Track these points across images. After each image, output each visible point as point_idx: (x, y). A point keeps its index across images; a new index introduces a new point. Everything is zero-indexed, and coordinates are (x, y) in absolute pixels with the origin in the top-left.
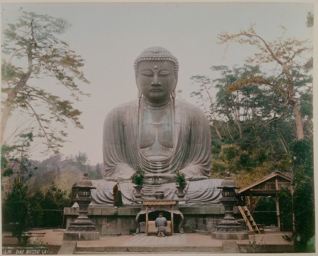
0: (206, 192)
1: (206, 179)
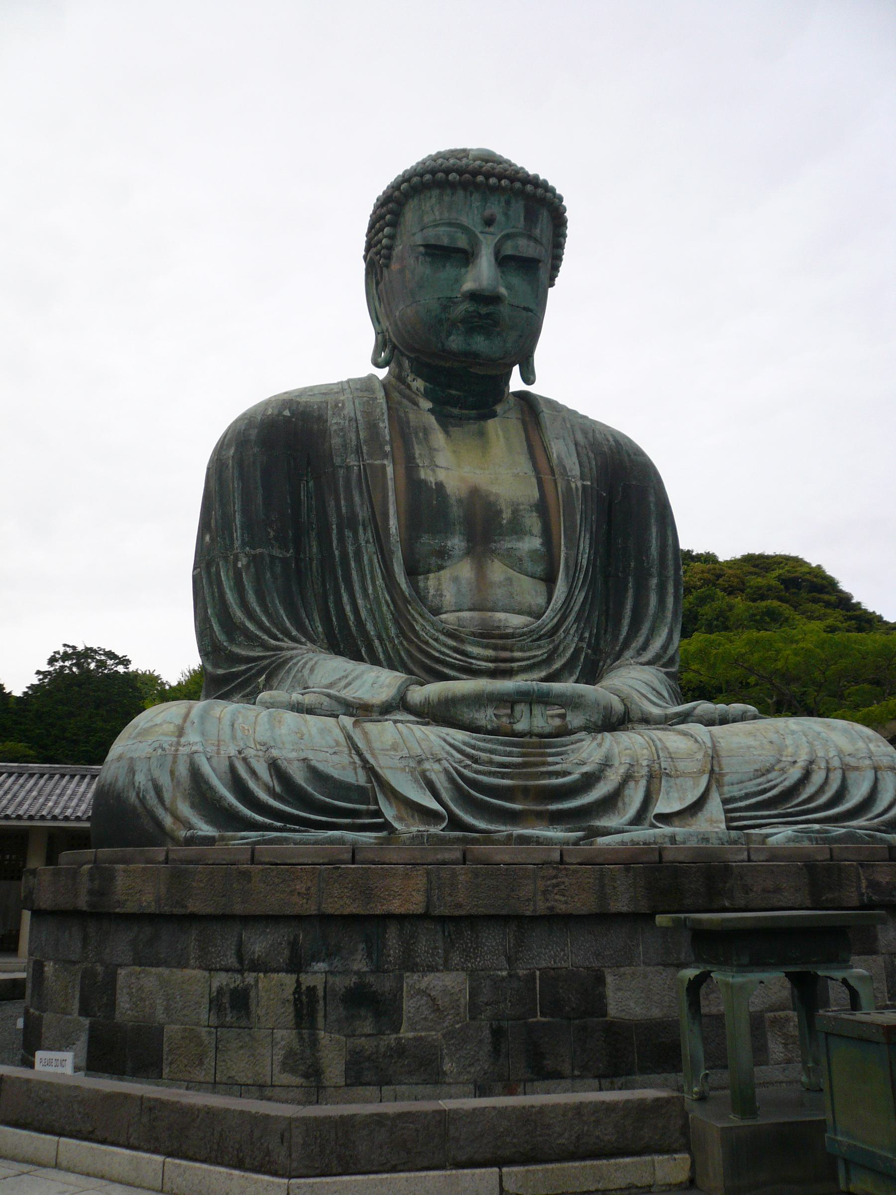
0: (807, 775)
1: (755, 718)
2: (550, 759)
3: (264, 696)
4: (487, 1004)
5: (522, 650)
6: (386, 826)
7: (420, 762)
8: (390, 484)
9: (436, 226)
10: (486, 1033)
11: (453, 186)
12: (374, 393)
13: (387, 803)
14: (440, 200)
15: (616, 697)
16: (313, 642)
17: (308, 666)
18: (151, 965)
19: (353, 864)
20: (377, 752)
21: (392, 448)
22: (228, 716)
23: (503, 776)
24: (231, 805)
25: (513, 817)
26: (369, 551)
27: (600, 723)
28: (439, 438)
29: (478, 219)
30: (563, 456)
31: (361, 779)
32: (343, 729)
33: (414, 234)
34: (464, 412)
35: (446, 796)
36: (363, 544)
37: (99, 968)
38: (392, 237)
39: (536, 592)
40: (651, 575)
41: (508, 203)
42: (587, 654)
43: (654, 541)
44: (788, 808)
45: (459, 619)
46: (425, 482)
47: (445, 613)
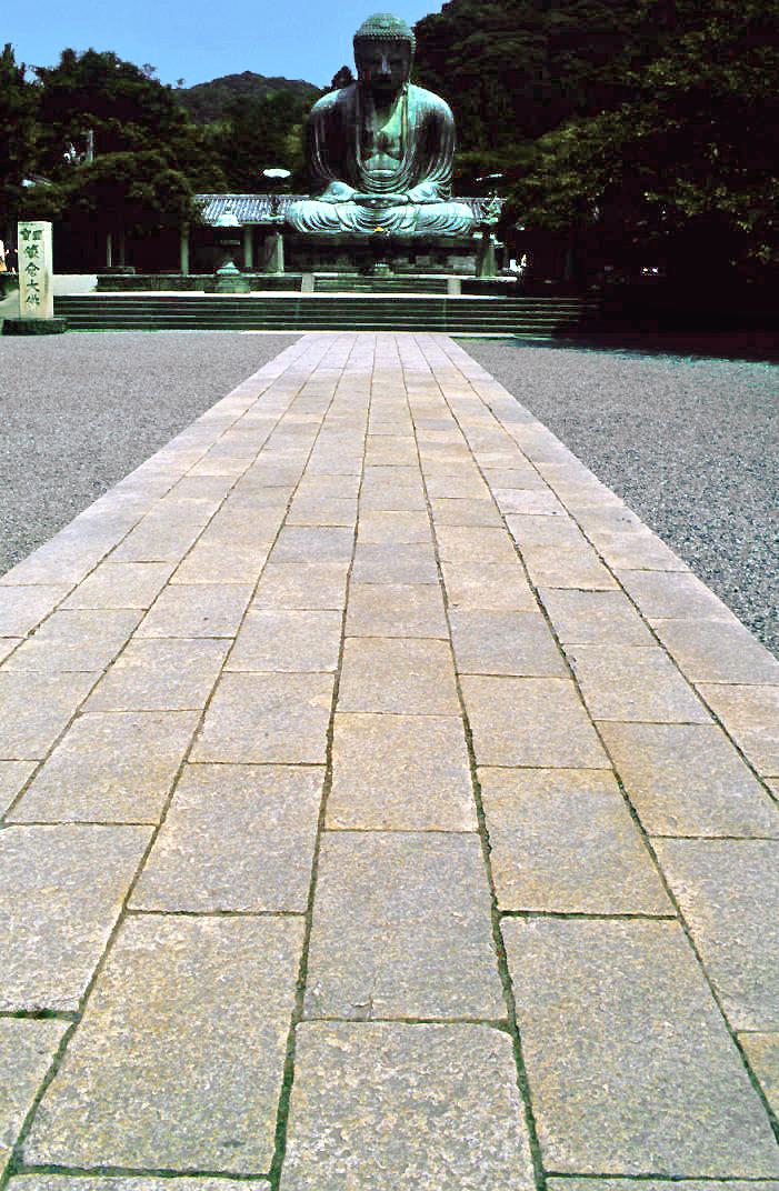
28: (374, 114)
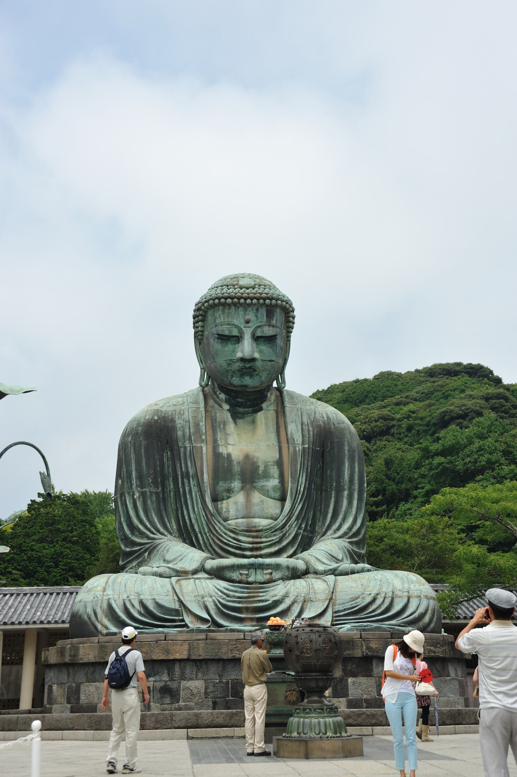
0: (374, 600)
1: (369, 571)
2: (261, 594)
3: (141, 569)
4: (211, 692)
5: (266, 537)
6: (186, 626)
7: (203, 598)
8: (204, 456)
9: (222, 325)
10: (211, 703)
11: (229, 305)
12: (199, 404)
13: (187, 616)
14: (223, 311)
15: (303, 562)
16: (171, 534)
17: (166, 549)
18: (93, 682)
19: (165, 640)
20: (184, 594)
21: (206, 437)
22: (124, 582)
23: (239, 602)
24: (123, 620)
25: (240, 620)
26: (194, 490)
27: (290, 576)
28: (231, 426)
29: (242, 321)
30: (294, 433)
31: (176, 606)
32: (172, 584)
33: (212, 328)
34: (246, 409)
35: (212, 612)
36: (192, 486)
37: (74, 685)
38: (203, 327)
39: (276, 507)
40: (344, 489)
41: (257, 310)
42: (303, 536)
43: (346, 471)
44: (362, 615)
45: (236, 523)
46: (221, 454)
47: (230, 520)
